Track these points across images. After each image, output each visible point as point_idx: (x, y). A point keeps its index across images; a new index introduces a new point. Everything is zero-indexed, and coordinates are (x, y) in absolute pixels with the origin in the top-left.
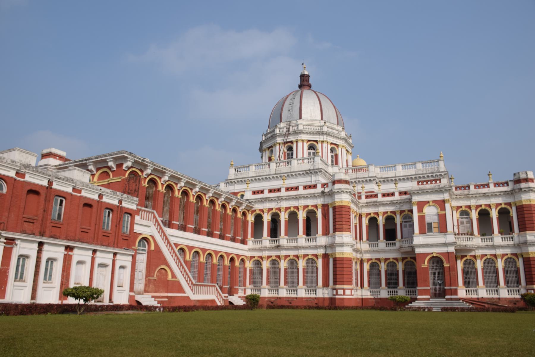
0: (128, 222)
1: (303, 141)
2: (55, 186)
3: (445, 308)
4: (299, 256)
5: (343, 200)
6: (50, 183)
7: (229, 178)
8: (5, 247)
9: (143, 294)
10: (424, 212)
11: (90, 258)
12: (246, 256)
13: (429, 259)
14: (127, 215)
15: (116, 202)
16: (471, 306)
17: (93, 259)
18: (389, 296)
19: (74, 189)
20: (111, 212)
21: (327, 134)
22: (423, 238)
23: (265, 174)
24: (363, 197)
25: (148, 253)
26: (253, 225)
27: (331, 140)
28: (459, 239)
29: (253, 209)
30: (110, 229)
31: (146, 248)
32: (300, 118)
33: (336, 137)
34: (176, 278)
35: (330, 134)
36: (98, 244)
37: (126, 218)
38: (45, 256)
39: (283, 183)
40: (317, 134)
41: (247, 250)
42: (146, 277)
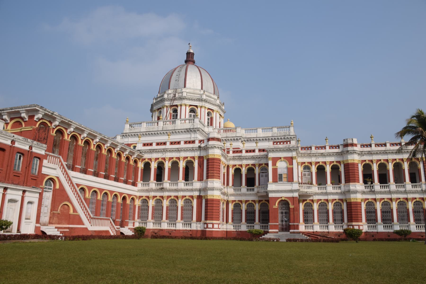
0: (36, 164)
1: (186, 105)
3: (289, 239)
4: (163, 196)
5: (215, 153)
7: (124, 132)
9: (47, 225)
10: (277, 166)
11: (2, 194)
12: (136, 196)
13: (278, 202)
14: (36, 159)
15: (27, 148)
16: (308, 238)
17: (4, 195)
18: (248, 229)
20: (22, 156)
21: (206, 101)
22: (275, 186)
23: (154, 130)
24: (231, 152)
25: (53, 191)
26: (143, 171)
27: (208, 106)
29: (143, 158)
30: (20, 170)
31: (52, 187)
32: (185, 87)
35: (208, 101)
36: (9, 183)
37: (36, 161)
39: (168, 138)
40: (198, 101)
41: (137, 190)
42: (51, 211)
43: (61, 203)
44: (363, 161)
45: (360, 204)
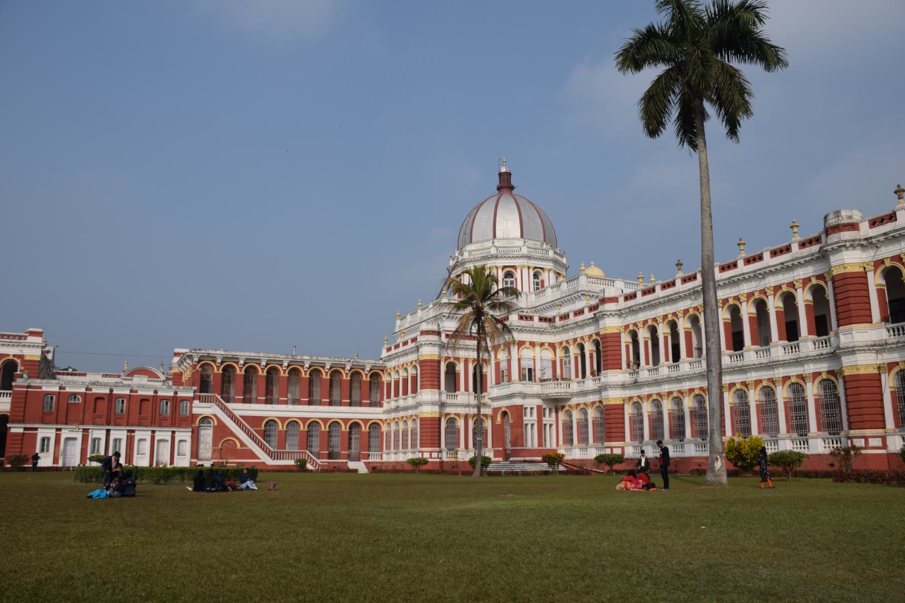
0: (187, 407)
2: (115, 392)
5: (424, 353)
6: (111, 391)
8: (83, 435)
12: (381, 420)
14: (185, 402)
15: (172, 394)
17: (153, 438)
19: (131, 391)
21: (496, 257)
23: (415, 323)
28: (559, 386)
30: (169, 413)
31: (212, 425)
32: (471, 242)
33: (509, 257)
34: (246, 446)
36: (157, 426)
37: (185, 404)
38: (112, 437)
43: (222, 438)
44: (627, 327)
45: (621, 407)
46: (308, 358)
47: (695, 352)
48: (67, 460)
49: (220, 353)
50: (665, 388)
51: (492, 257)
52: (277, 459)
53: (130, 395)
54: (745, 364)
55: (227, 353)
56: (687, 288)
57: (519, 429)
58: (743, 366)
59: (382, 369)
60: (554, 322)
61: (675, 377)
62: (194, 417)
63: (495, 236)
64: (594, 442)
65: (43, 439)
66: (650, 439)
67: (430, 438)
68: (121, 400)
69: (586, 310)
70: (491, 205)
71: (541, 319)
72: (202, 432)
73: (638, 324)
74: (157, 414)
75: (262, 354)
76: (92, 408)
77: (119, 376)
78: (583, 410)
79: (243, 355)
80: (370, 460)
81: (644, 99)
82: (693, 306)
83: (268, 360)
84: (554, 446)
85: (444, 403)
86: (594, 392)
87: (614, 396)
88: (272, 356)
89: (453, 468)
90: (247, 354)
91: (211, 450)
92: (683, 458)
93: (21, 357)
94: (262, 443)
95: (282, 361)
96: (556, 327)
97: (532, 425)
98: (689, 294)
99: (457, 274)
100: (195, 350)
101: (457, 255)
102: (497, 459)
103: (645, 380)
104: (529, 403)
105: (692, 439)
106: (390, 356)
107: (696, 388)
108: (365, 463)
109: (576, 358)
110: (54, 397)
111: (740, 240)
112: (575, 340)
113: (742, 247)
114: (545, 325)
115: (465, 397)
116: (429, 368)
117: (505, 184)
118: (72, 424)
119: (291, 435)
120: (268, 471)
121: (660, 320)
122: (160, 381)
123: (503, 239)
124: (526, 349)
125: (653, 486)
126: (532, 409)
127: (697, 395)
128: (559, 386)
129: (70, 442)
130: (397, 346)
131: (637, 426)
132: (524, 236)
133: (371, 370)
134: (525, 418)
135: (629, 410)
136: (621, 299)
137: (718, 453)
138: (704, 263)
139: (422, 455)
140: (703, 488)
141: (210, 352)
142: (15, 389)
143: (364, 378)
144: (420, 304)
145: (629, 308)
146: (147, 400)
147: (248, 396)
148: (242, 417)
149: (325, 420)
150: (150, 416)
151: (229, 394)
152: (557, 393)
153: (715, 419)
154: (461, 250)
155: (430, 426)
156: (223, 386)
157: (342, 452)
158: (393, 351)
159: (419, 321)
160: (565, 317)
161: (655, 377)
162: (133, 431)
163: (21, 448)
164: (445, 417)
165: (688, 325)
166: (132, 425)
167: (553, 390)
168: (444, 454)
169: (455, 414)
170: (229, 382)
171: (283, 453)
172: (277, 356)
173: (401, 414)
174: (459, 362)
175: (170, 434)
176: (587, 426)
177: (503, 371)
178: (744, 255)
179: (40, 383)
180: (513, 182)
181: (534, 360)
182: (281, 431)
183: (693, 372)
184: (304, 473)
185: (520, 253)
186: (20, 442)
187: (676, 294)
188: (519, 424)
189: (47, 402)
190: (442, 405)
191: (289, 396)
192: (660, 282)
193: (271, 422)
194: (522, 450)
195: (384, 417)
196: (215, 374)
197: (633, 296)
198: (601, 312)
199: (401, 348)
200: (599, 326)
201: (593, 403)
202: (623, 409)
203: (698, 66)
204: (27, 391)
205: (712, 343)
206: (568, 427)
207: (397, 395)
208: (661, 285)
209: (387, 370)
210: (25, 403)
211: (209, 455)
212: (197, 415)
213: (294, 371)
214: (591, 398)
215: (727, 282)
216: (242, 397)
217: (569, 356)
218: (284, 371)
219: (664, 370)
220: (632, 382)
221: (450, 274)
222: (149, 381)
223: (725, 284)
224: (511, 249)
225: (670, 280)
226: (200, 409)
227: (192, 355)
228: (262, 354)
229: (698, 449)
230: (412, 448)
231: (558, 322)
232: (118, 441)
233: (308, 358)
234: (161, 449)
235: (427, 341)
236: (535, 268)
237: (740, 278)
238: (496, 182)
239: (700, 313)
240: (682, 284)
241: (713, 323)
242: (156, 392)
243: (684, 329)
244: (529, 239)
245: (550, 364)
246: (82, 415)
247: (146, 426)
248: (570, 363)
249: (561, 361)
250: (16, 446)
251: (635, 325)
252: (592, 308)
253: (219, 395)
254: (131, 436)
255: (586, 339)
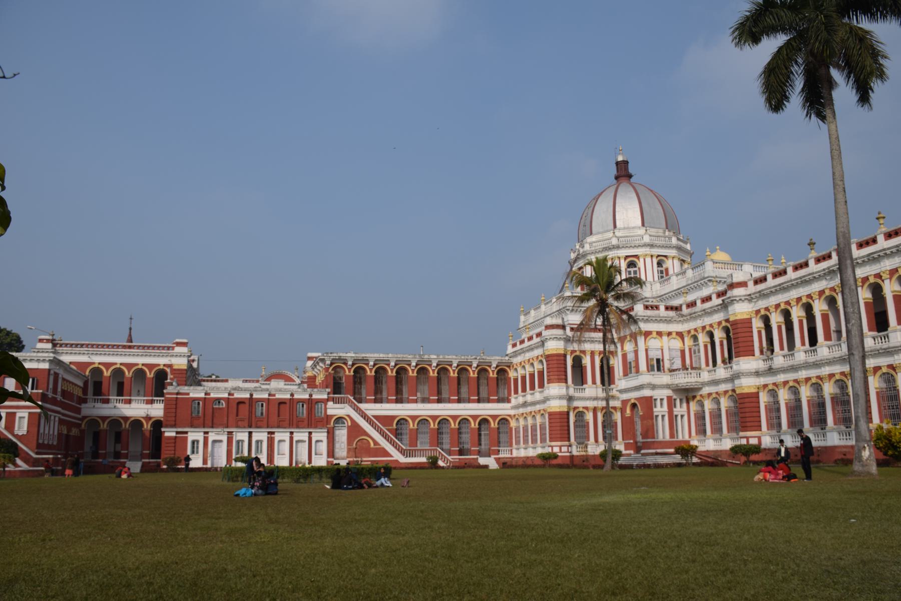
2: (255, 396)
5: (549, 348)
6: (251, 395)
8: (228, 437)
12: (509, 416)
14: (320, 404)
15: (307, 397)
17: (291, 439)
19: (270, 395)
23: (539, 318)
28: (689, 375)
31: (346, 425)
32: (591, 234)
33: (631, 246)
34: (379, 445)
36: (294, 428)
37: (320, 406)
38: (254, 439)
44: (758, 312)
45: (756, 396)
46: (435, 357)
47: (834, 336)
48: (215, 461)
49: (350, 356)
50: (803, 374)
51: (614, 248)
52: (410, 457)
53: (268, 399)
54: (891, 345)
55: (357, 355)
56: (822, 268)
57: (650, 421)
58: (889, 348)
59: (509, 365)
60: (681, 310)
61: (813, 362)
62: (328, 418)
63: (615, 226)
64: (728, 432)
65: (193, 442)
66: (789, 427)
67: (559, 432)
68: (260, 403)
69: (714, 297)
70: (609, 194)
71: (667, 308)
72: (337, 432)
73: (770, 308)
74: (295, 416)
75: (390, 355)
76: (235, 411)
77: (258, 381)
78: (716, 400)
79: (372, 357)
80: (501, 456)
81: (764, 72)
82: (829, 286)
83: (397, 360)
84: (687, 438)
85: (571, 397)
86: (726, 380)
87: (747, 384)
88: (400, 356)
89: (584, 461)
90: (377, 355)
91: (346, 450)
92: (826, 448)
93: (170, 366)
94: (394, 441)
95: (410, 361)
96: (683, 316)
97: (663, 416)
98: (824, 274)
99: (579, 266)
100: (327, 353)
101: (578, 247)
102: (628, 452)
103: (780, 366)
104: (659, 394)
105: (835, 427)
106: (516, 351)
107: (837, 373)
108: (495, 458)
109: (706, 346)
110: (201, 403)
111: (879, 213)
112: (704, 328)
113: (882, 221)
114: (672, 314)
115: (592, 391)
116: (555, 362)
117: (623, 172)
118: (217, 427)
119: (422, 433)
120: (402, 468)
121: (793, 303)
122: (296, 385)
123: (624, 228)
124: (653, 340)
125: (795, 477)
126: (662, 400)
127: (838, 381)
128: (689, 375)
129: (217, 444)
130: (522, 342)
131: (774, 414)
132: (646, 224)
133: (497, 366)
134: (655, 410)
135: (764, 398)
136: (751, 284)
137: (866, 441)
138: (839, 241)
139: (552, 449)
140: (850, 478)
141: (341, 355)
142: (167, 396)
143: (491, 375)
144: (543, 298)
145: (760, 292)
146: (285, 403)
147: (379, 396)
148: (374, 416)
149: (454, 417)
150: (288, 417)
151: (361, 395)
152: (687, 383)
153: (860, 406)
154: (581, 242)
155: (558, 420)
156: (355, 387)
157: (473, 449)
158: (519, 347)
159: (543, 316)
160: (692, 304)
161: (791, 363)
162: (273, 433)
163: (175, 450)
164: (574, 411)
165: (825, 307)
166: (272, 427)
167: (684, 379)
168: (574, 448)
169: (583, 408)
170: (360, 383)
171: (415, 450)
172: (405, 356)
173: (529, 409)
174: (585, 355)
175: (307, 434)
176: (720, 416)
177: (630, 363)
178: (884, 229)
179: (188, 390)
180: (631, 170)
181: (662, 350)
182: (412, 429)
183: (833, 356)
184: (436, 470)
185: (642, 242)
186: (173, 445)
187: (810, 274)
188: (649, 416)
189: (195, 408)
190: (570, 399)
191: (419, 395)
192: (792, 263)
193: (402, 421)
194: (654, 442)
195: (512, 412)
196: (347, 377)
197: (763, 279)
198: (729, 298)
199: (527, 344)
200: (728, 312)
201: (726, 392)
202: (758, 397)
203: (822, 32)
204: (177, 398)
205: (853, 325)
206: (701, 417)
207: (524, 390)
208: (793, 266)
209: (513, 366)
210: (176, 408)
211: (344, 454)
212: (332, 416)
213: (422, 371)
214: (723, 387)
215: (866, 259)
216: (374, 398)
217: (698, 345)
218: (413, 371)
219: (801, 355)
220: (767, 369)
221: (572, 267)
222: (285, 384)
223: (863, 261)
224: (633, 238)
225: (802, 261)
226: (335, 410)
227: (324, 359)
228: (390, 355)
229: (842, 437)
230: (541, 442)
231: (685, 310)
232: (260, 443)
233: (435, 357)
234: (299, 449)
235: (552, 335)
236: (659, 256)
237: (881, 254)
238: (614, 171)
239: (837, 294)
240: (816, 264)
241: (852, 303)
242: (292, 395)
243: (821, 311)
244: (650, 227)
245: (679, 354)
246: (226, 418)
247: (285, 428)
248: (699, 352)
249: (690, 349)
250: (169, 448)
251: (767, 309)
252: (720, 294)
253: (351, 396)
254: (271, 437)
255: (715, 326)
